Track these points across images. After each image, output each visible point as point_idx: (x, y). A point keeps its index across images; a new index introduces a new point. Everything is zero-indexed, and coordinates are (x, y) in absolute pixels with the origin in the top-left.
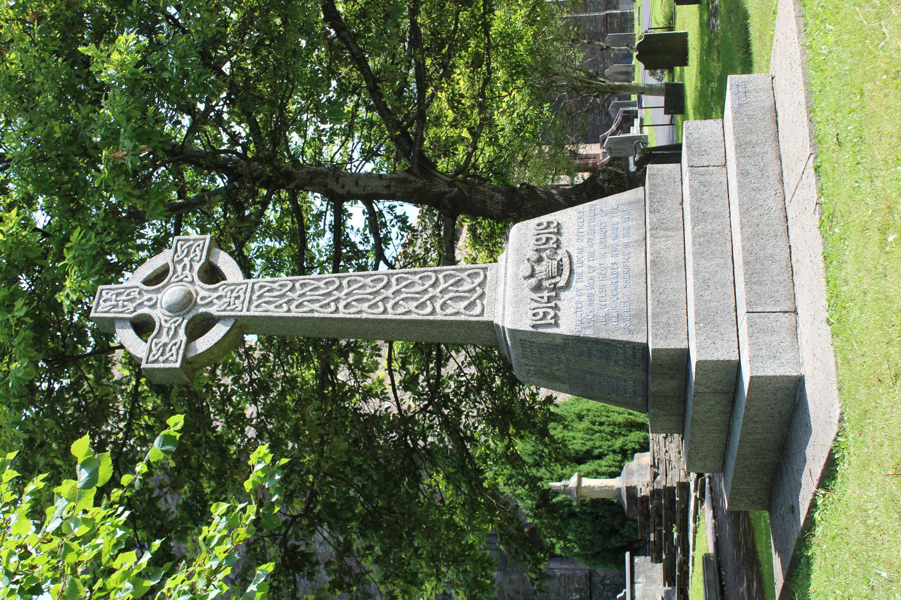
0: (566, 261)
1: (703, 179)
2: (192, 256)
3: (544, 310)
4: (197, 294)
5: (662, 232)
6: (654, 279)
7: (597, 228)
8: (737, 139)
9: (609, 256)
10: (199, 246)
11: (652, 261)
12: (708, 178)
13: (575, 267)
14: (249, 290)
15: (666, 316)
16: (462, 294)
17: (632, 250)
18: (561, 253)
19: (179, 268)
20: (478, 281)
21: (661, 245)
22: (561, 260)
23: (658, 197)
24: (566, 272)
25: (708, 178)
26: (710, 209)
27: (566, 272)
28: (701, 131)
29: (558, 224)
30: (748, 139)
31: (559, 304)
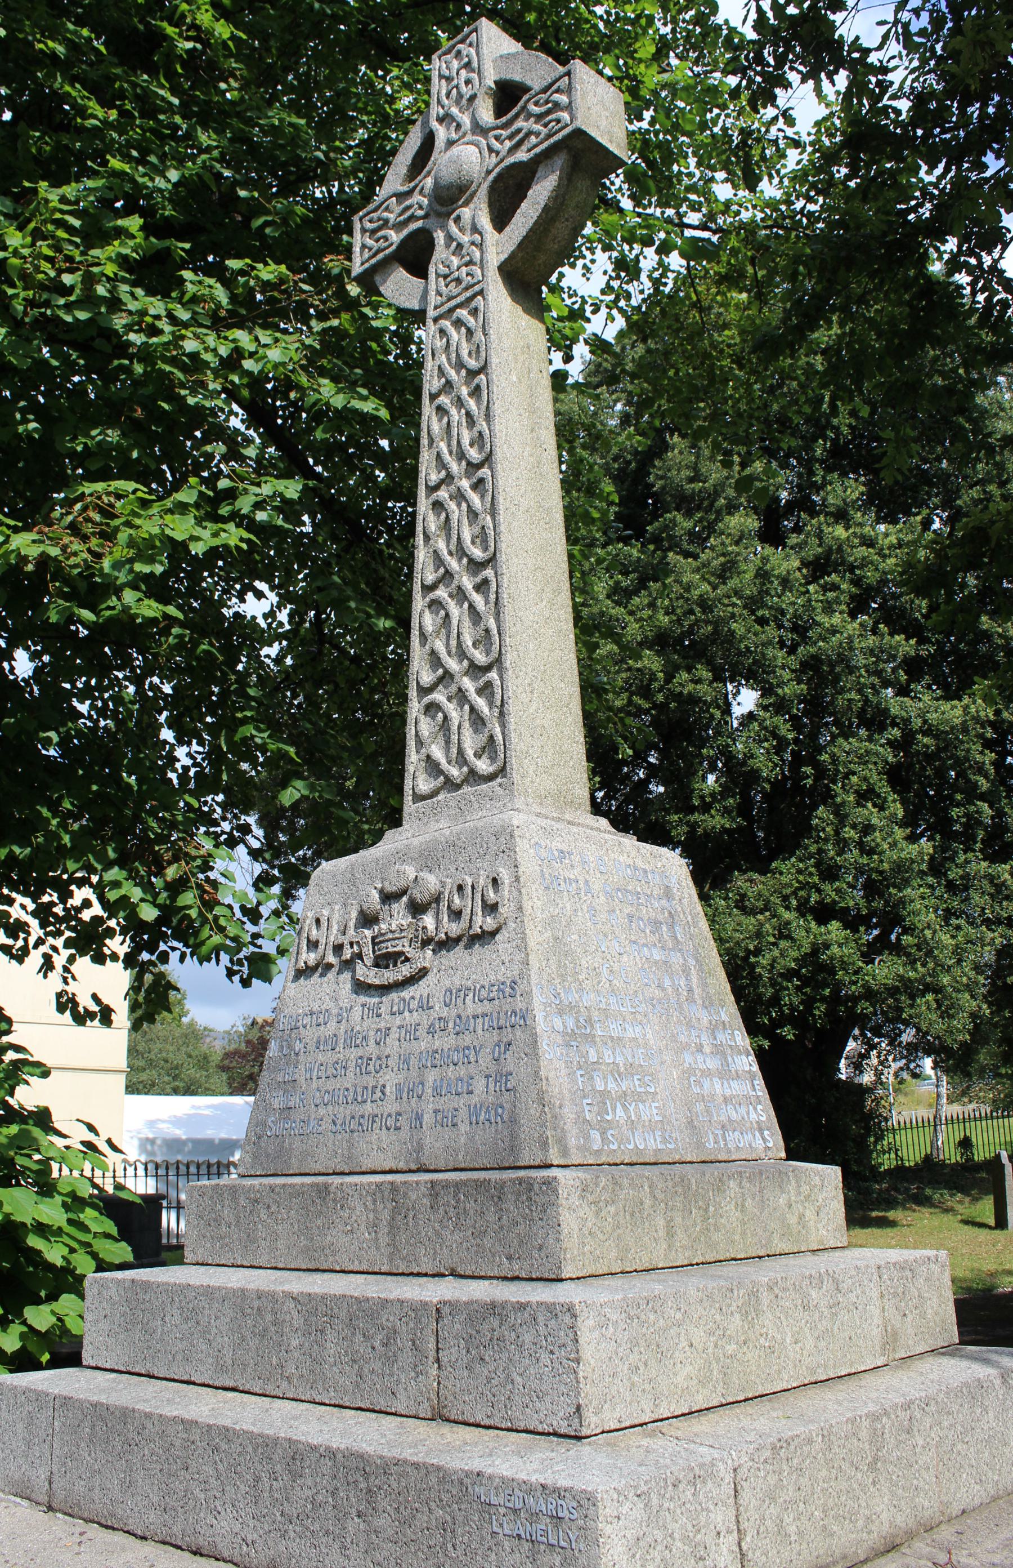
0: (405, 971)
1: (403, 1341)
2: (538, 127)
3: (323, 941)
4: (466, 204)
5: (386, 1215)
6: (298, 1192)
7: (467, 1039)
8: (388, 1467)
9: (400, 1079)
10: (558, 121)
11: (326, 1186)
12: (407, 1358)
13: (394, 995)
14: (468, 294)
15: (232, 1219)
16: (455, 738)
17: (405, 1134)
18: (426, 957)
19: (520, 123)
20: (483, 766)
21: (359, 1211)
22: (407, 959)
23: (471, 1205)
24: (389, 976)
25: (407, 1358)
26: (331, 1349)
27: (389, 976)
28: (545, 1358)
29: (493, 934)
30: (384, 1504)
31: (331, 975)
